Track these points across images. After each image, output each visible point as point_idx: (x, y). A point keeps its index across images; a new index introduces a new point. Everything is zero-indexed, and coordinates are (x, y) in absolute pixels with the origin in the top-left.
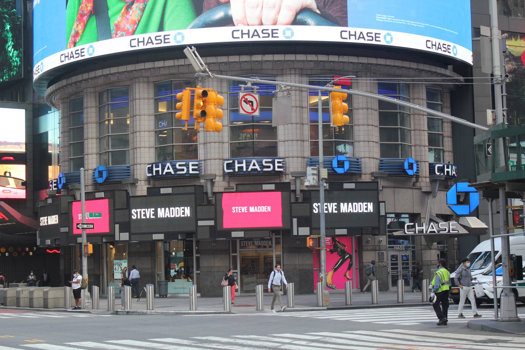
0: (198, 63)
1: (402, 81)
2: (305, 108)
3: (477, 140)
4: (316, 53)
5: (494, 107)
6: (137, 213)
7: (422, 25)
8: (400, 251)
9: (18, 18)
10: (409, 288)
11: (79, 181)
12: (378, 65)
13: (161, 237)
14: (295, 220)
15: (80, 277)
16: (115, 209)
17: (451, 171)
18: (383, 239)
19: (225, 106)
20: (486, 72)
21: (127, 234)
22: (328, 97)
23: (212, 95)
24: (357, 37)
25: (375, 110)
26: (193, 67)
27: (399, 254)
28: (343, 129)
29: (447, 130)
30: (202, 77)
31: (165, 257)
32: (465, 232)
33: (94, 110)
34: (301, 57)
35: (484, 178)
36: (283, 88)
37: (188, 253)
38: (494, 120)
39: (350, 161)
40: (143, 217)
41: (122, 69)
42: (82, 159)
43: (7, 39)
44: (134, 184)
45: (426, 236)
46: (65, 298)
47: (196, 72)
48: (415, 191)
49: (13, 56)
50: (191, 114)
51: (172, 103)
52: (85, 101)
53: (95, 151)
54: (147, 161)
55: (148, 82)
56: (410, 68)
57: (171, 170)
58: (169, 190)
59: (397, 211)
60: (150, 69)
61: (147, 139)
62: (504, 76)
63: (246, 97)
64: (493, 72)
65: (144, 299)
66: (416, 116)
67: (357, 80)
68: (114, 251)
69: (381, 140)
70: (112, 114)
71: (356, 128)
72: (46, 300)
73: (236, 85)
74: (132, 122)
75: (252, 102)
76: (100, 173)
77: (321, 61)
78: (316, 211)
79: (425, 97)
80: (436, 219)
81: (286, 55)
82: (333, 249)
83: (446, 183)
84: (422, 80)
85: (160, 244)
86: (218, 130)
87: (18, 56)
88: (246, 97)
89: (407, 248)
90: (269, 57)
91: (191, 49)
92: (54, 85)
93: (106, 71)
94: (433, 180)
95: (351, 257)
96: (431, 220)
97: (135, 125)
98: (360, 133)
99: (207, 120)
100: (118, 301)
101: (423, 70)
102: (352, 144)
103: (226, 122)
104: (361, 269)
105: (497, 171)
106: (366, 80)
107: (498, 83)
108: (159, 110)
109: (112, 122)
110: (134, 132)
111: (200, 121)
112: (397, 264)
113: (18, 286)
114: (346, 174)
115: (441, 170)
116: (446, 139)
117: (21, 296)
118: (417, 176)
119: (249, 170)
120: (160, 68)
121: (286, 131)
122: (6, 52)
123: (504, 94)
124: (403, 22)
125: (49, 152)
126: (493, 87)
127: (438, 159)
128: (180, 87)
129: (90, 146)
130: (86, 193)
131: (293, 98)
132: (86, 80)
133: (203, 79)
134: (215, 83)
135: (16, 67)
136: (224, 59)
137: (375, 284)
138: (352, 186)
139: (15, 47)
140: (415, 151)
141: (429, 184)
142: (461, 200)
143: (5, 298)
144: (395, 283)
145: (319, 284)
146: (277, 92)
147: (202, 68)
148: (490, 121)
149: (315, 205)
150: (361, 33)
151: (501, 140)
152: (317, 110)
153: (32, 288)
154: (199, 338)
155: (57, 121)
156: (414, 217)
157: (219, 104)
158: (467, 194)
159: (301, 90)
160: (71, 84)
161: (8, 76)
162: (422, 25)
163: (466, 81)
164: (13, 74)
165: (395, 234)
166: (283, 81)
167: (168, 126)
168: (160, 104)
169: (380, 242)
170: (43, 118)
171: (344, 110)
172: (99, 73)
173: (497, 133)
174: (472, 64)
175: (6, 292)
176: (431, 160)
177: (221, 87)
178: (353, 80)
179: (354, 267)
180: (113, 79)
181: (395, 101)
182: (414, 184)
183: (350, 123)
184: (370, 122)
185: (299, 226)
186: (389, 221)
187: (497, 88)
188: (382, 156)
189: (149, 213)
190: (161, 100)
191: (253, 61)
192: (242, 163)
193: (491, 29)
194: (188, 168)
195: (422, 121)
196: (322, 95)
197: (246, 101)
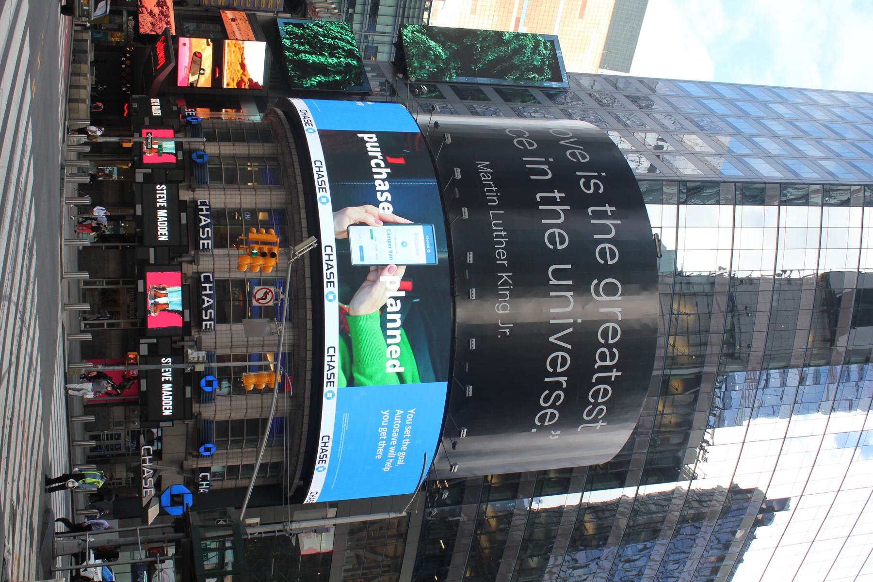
0: (304, 248)
1: (287, 439)
3: (231, 510)
4: (313, 359)
6: (162, 191)
7: (340, 456)
8: (125, 441)
10: (88, 451)
11: (193, 136)
13: (139, 212)
14: (155, 341)
15: (99, 133)
16: (166, 169)
17: (204, 488)
18: (137, 425)
19: (264, 275)
21: (142, 181)
23: (272, 262)
27: (121, 442)
29: (241, 483)
30: (289, 253)
31: (118, 216)
32: (144, 503)
33: (261, 152)
34: (309, 344)
35: (194, 519)
37: (122, 238)
38: (250, 525)
39: (212, 392)
40: (158, 196)
42: (214, 140)
44: (191, 188)
45: (139, 467)
46: (79, 119)
48: (183, 455)
50: (257, 243)
51: (267, 225)
52: (270, 144)
53: (223, 152)
54: (212, 201)
55: (286, 203)
57: (203, 223)
58: (184, 221)
59: (164, 438)
61: (233, 201)
65: (76, 195)
68: (125, 167)
71: (243, 397)
72: (77, 101)
74: (250, 187)
76: (201, 157)
78: (163, 360)
79: (274, 460)
80: (157, 476)
82: (126, 378)
83: (192, 483)
84: (286, 458)
85: (132, 211)
86: (239, 267)
87: (311, 85)
89: (128, 448)
90: (309, 315)
93: (297, 165)
94: (196, 471)
95: (118, 395)
96: (155, 471)
98: (240, 401)
100: (75, 170)
102: (229, 394)
103: (249, 275)
104: (106, 405)
105: (201, 530)
110: (239, 189)
112: (112, 439)
113: (92, 75)
114: (200, 389)
115: (205, 478)
116: (234, 482)
117: (82, 78)
118: (199, 456)
120: (300, 214)
122: (315, 75)
124: (342, 438)
125: (224, 110)
127: (214, 475)
128: (281, 232)
129: (227, 148)
130: (182, 142)
131: (272, 338)
132: (289, 146)
137: (92, 418)
138: (188, 395)
139: (319, 83)
140: (222, 454)
141: (190, 467)
142: (175, 499)
143: (80, 63)
144: (93, 438)
145: (91, 365)
149: (170, 360)
151: (231, 532)
152: (260, 360)
153: (89, 88)
154: (35, 247)
156: (158, 455)
158: (181, 503)
159: (279, 346)
160: (285, 132)
162: (340, 456)
165: (142, 437)
169: (134, 422)
171: (258, 385)
172: (295, 158)
173: (238, 529)
175: (86, 63)
176: (213, 469)
179: (108, 398)
180: (290, 171)
181: (268, 433)
182: (190, 453)
184: (249, 411)
185: (149, 345)
186: (155, 431)
188: (217, 422)
189: (162, 202)
190: (270, 216)
194: (205, 239)
197: (266, 294)
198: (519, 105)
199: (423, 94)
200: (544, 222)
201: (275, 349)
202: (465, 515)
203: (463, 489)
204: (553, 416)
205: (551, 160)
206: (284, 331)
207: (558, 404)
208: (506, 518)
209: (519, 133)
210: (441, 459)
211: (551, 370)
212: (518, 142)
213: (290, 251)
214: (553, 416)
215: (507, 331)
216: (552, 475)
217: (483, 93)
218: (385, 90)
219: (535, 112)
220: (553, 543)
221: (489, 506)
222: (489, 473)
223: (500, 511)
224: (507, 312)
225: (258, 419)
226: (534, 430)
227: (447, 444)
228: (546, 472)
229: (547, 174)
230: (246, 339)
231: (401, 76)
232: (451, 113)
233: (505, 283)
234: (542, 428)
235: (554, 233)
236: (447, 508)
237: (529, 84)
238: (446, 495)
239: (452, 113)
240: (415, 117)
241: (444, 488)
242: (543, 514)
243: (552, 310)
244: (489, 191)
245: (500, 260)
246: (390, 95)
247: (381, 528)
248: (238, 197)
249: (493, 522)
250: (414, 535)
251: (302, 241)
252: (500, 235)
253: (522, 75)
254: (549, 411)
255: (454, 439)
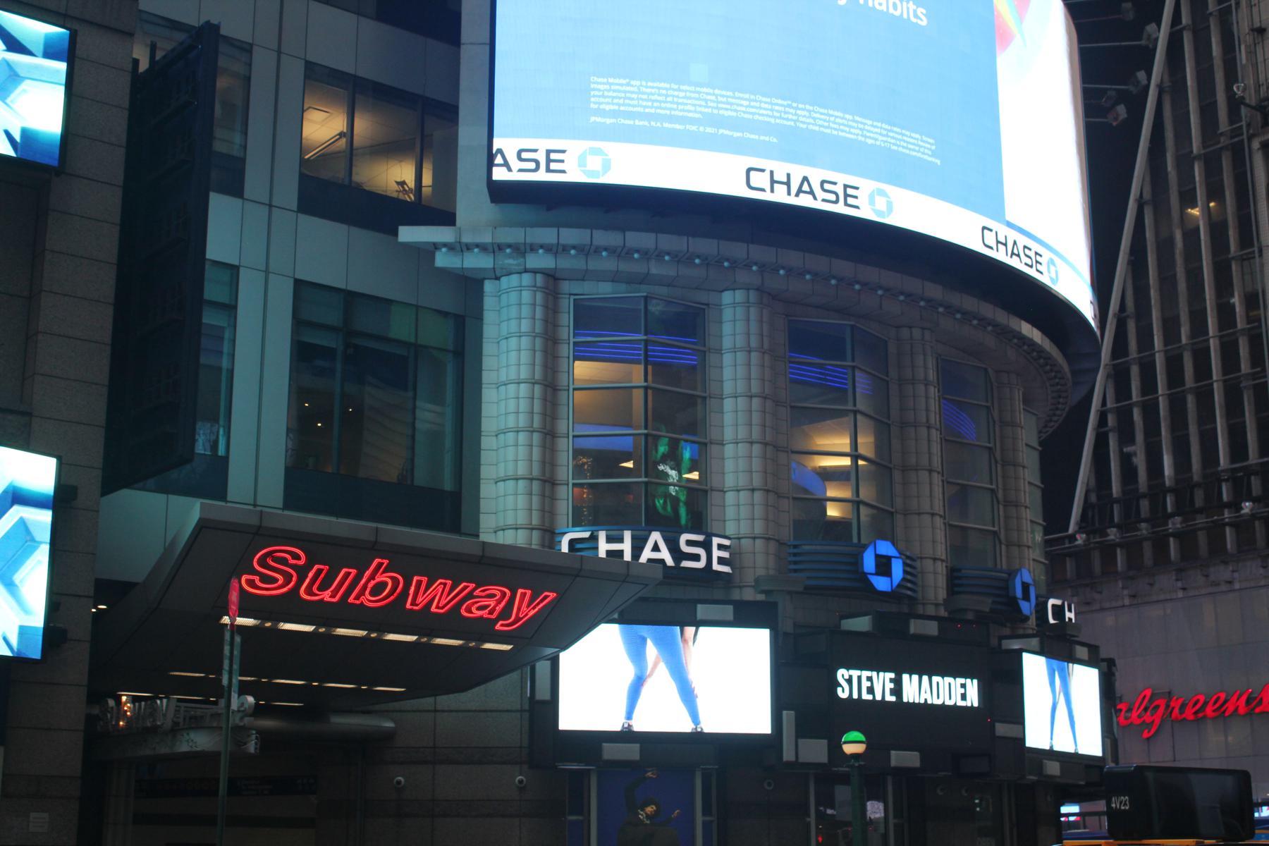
24: (794, 190)
119: (643, 559)
150: (805, 179)
192: (621, 540)
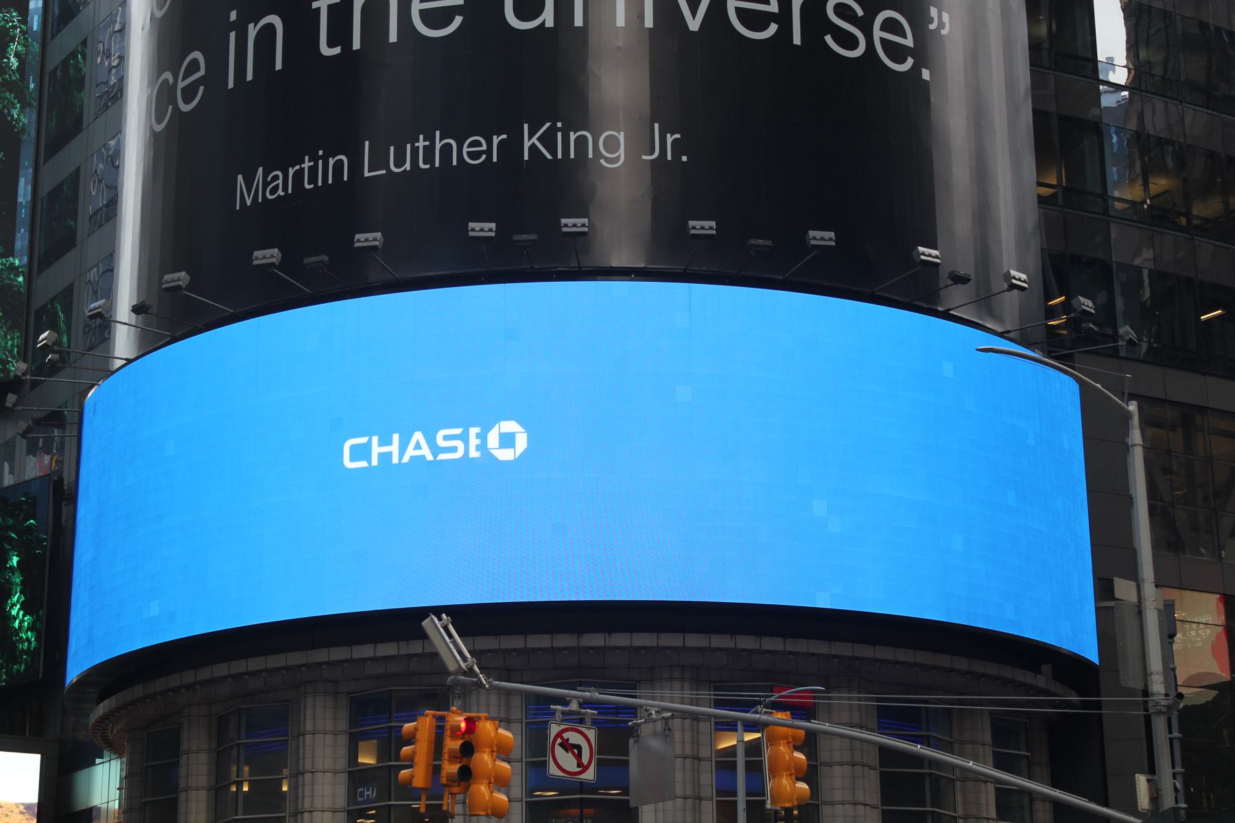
0: (454, 650)
2: (706, 759)
5: (1151, 770)
9: (40, 541)
12: (877, 660)
19: (516, 753)
20: (1131, 685)
22: (759, 735)
23: (487, 728)
25: (870, 768)
26: (441, 661)
28: (796, 812)
33: (203, 757)
34: (695, 640)
36: (654, 716)
38: (1155, 799)
41: (274, 661)
43: (11, 589)
47: (449, 674)
49: (20, 627)
50: (436, 770)
51: (391, 744)
56: (951, 670)
60: (341, 662)
62: (1173, 695)
63: (566, 735)
64: (1146, 686)
66: (970, 784)
67: (829, 698)
69: (884, 801)
70: (246, 769)
71: (826, 810)
73: (542, 704)
74: (294, 787)
75: (579, 747)
77: (744, 650)
79: (988, 737)
81: (663, 635)
84: (980, 703)
88: (566, 735)
90: (621, 640)
91: (440, 619)
92: (113, 698)
93: (239, 666)
97: (300, 795)
99: (473, 787)
101: (983, 675)
103: (517, 791)
106: (850, 699)
107: (1159, 713)
108: (360, 760)
109: (246, 789)
111: (456, 790)
120: (364, 660)
121: (661, 814)
123: (1176, 734)
126: (1148, 720)
128: (411, 710)
131: (677, 735)
132: (190, 687)
133: (467, 691)
134: (494, 698)
135: (25, 652)
136: (516, 642)
146: (639, 725)
147: (463, 665)
148: (1144, 801)
152: (733, 766)
155: (115, 783)
157: (502, 752)
159: (696, 718)
161: (7, 674)
163: (1085, 705)
164: (18, 671)
166: (654, 699)
167: (378, 799)
168: (362, 745)
170: (82, 775)
171: (798, 768)
172: (221, 670)
174: (1094, 657)
177: (508, 707)
178: (819, 698)
181: (918, 748)
183: (812, 797)
184: (860, 798)
187: (1159, 725)
190: (365, 736)
191: (584, 648)
193: (1138, 587)
195: (983, 797)
196: (746, 731)
197: (566, 746)
198: (89, 98)
199: (58, 343)
200: (393, 38)
201: (705, 727)
202: (1138, 253)
203: (1069, 260)
204: (889, 25)
205: (233, 16)
206: (657, 703)
207: (860, 12)
208: (1149, 151)
209: (163, 97)
210: (992, 314)
211: (773, 28)
212: (187, 101)
213: (457, 684)
214: (889, 25)
215: (670, 139)
216: (1043, 30)
217: (58, 189)
218: (49, 441)
219: (108, 54)
220: (1218, 29)
221: (1117, 194)
222: (1032, 191)
223: (1131, 167)
224: (621, 137)
225: (883, 776)
226: (926, 74)
227: (956, 297)
228: (1035, 46)
229: (270, 28)
230: (679, 801)
231: (11, 399)
232: (110, 271)
233: (549, 140)
234: (922, 52)
235: (422, 12)
236: (1119, 303)
237: (34, 62)
238: (1087, 304)
239: (111, 270)
240: (119, 363)
241: (1066, 307)
242: (1143, 55)
243: (621, 21)
244: (313, 179)
245: (489, 152)
246: (62, 426)
247: (1167, 471)
248: (317, 815)
249: (1159, 184)
250: (1186, 387)
251: (436, 655)
252: (426, 151)
253: (9, 86)
254: (878, 34)
255: (944, 280)
